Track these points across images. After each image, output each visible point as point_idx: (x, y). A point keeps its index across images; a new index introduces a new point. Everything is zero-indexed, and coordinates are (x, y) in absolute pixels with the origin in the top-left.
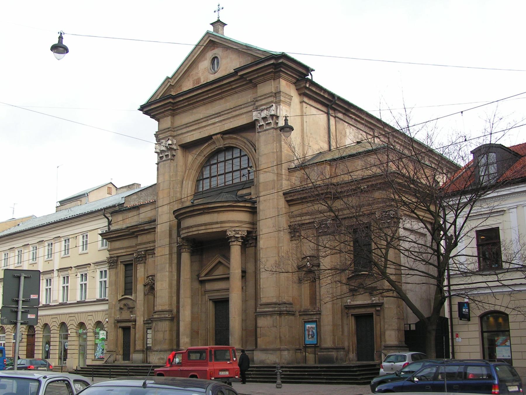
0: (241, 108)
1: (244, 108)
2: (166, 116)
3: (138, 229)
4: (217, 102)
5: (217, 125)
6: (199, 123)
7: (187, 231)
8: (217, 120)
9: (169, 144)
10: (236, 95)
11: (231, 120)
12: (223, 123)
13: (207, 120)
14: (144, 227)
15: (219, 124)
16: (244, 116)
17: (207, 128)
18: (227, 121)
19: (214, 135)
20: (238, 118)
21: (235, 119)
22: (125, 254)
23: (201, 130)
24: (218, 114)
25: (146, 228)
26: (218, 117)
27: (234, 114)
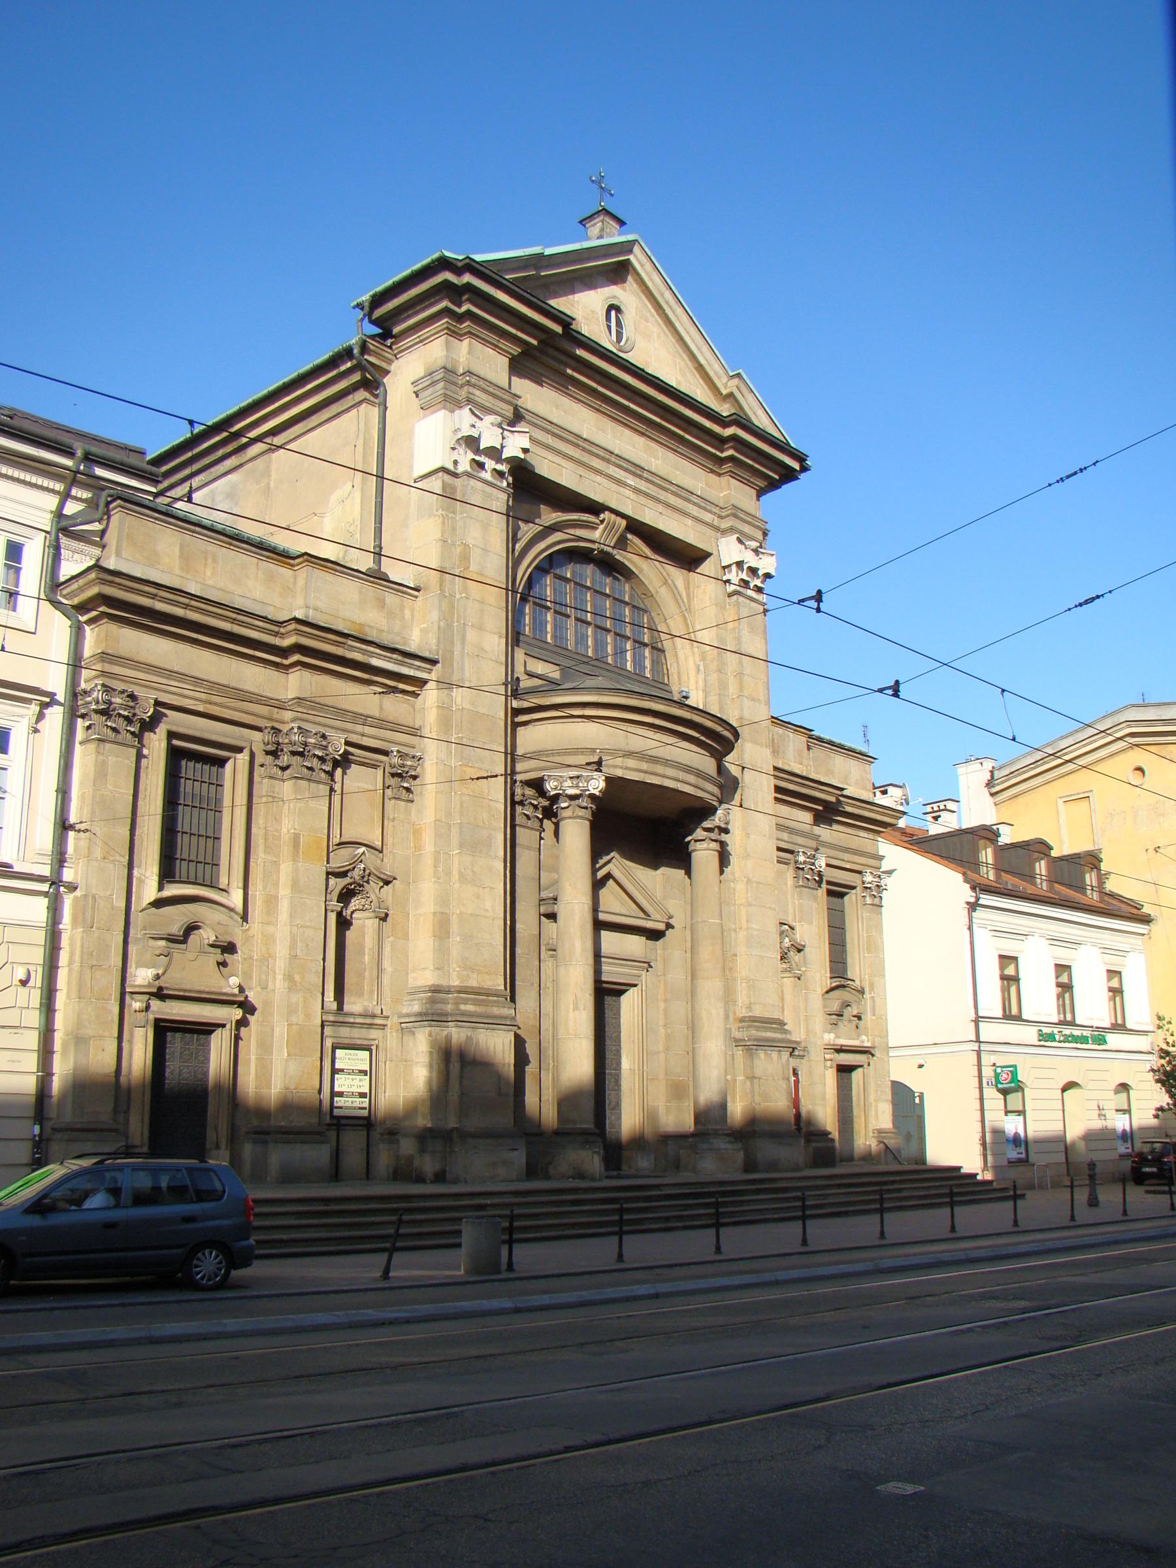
0: (688, 501)
1: (695, 504)
2: (495, 347)
3: (339, 651)
4: (627, 432)
5: (628, 493)
6: (584, 449)
7: (644, 766)
8: (631, 480)
9: (526, 451)
10: (671, 455)
11: (660, 508)
12: (643, 500)
13: (608, 461)
14: (372, 655)
15: (632, 496)
16: (689, 522)
17: (599, 479)
18: (650, 503)
19: (612, 511)
20: (676, 516)
21: (669, 512)
22: (201, 708)
23: (581, 471)
24: (637, 470)
25: (375, 662)
26: (634, 474)
27: (672, 500)
